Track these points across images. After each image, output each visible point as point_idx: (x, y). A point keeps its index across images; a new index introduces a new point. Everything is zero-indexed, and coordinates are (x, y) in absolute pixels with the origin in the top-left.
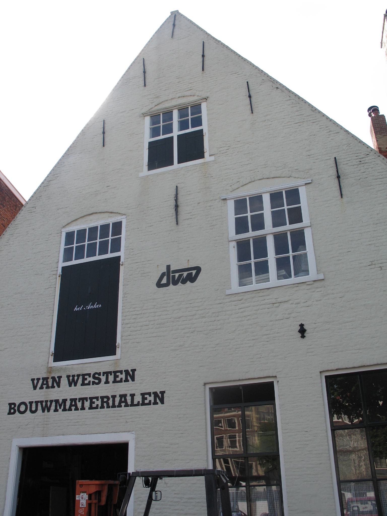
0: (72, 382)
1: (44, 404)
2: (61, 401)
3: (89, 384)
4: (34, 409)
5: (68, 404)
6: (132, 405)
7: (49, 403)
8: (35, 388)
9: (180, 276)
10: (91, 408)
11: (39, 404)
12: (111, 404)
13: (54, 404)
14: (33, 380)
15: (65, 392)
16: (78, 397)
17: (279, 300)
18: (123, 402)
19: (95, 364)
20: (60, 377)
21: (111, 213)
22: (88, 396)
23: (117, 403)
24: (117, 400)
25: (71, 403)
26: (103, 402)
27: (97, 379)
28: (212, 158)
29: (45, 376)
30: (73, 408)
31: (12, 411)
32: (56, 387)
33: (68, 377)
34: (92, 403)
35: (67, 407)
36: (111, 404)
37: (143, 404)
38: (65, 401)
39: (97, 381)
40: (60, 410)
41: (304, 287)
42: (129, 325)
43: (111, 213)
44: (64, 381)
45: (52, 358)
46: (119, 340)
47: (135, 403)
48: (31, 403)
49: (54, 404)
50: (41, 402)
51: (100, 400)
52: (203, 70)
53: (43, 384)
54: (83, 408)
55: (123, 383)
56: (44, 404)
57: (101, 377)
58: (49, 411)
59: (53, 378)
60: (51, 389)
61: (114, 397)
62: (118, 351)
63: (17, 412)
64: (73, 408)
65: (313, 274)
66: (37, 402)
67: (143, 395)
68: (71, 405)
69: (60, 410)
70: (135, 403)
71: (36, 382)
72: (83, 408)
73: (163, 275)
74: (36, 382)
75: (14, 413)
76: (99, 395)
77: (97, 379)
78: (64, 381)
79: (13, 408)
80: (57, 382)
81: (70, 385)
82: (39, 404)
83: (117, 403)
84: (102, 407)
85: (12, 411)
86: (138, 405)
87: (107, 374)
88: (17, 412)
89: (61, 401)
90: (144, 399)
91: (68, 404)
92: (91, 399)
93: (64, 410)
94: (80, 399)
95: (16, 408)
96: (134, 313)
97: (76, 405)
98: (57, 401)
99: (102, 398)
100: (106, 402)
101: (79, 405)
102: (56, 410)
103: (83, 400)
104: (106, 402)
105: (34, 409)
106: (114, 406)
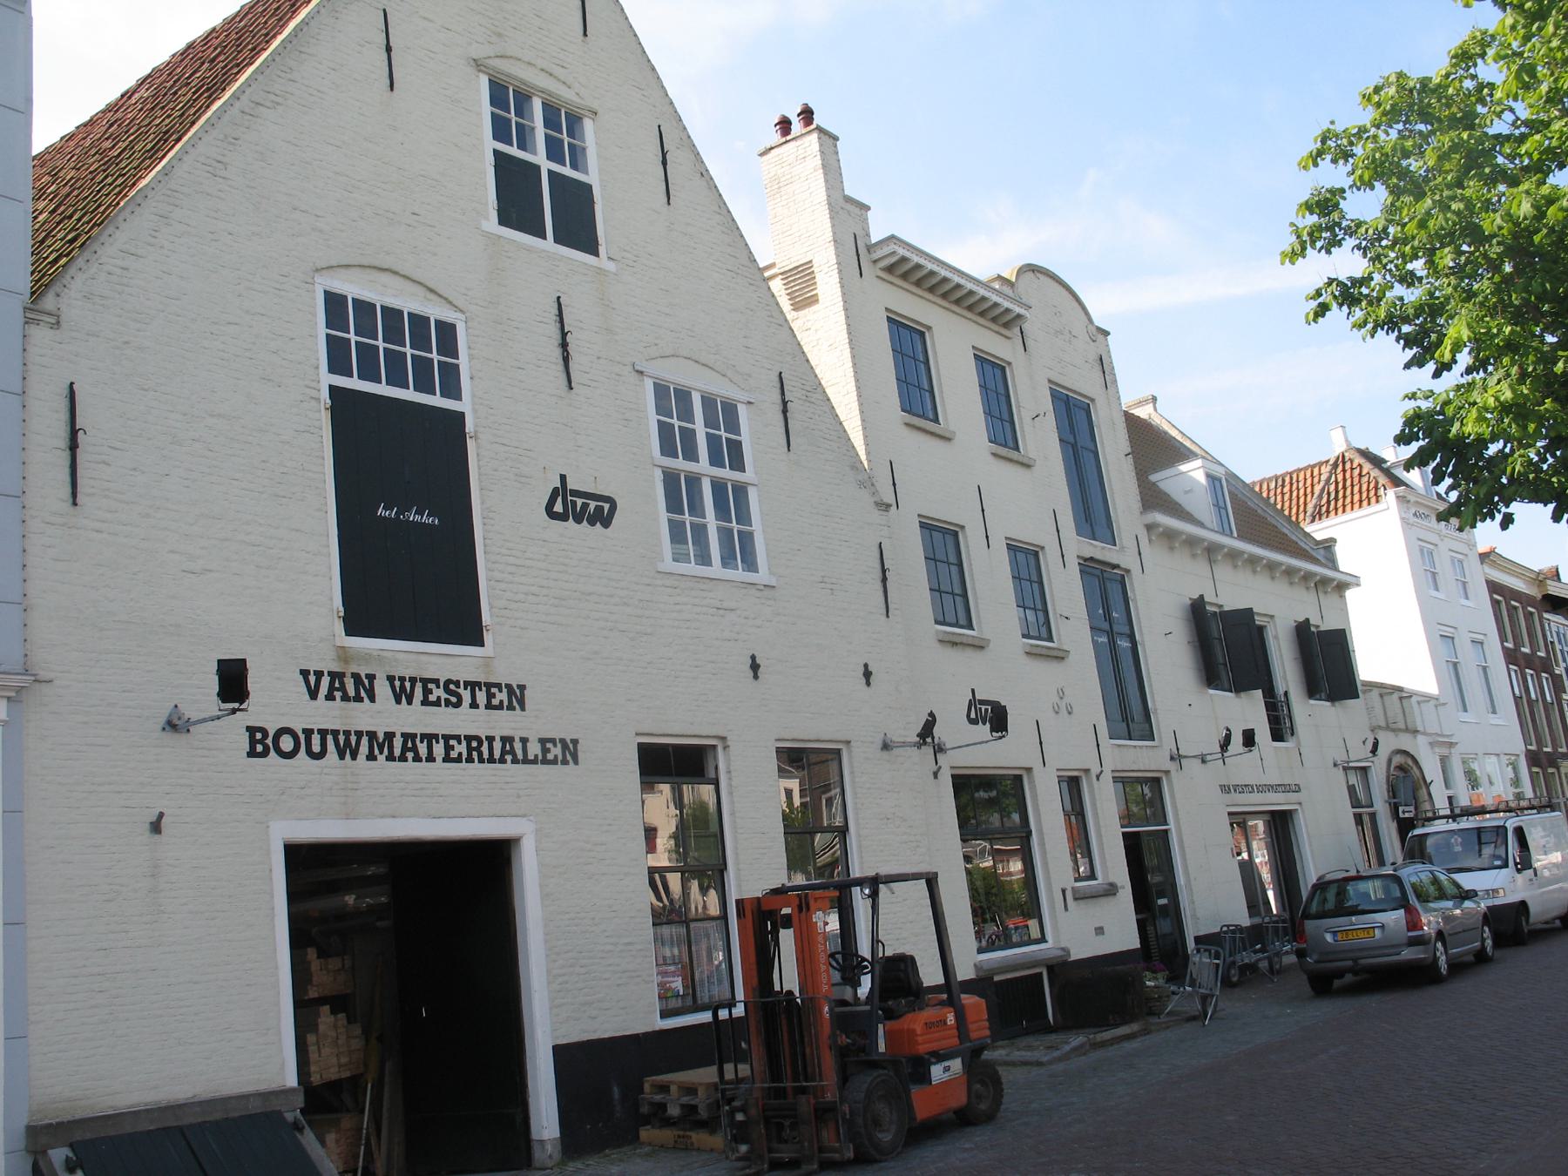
0: (402, 693)
1: (342, 738)
2: (381, 737)
3: (437, 703)
4: (316, 748)
5: (398, 743)
6: (526, 761)
7: (353, 739)
8: (313, 695)
9: (585, 506)
10: (447, 759)
11: (330, 738)
12: (486, 755)
13: (365, 741)
14: (305, 673)
15: (383, 715)
16: (418, 731)
17: (725, 605)
18: (410, 750)
19: (444, 659)
20: (371, 677)
21: (431, 291)
22: (441, 732)
23: (497, 754)
24: (497, 745)
25: (504, 747)
26: (470, 749)
27: (453, 692)
28: (611, 266)
29: (336, 668)
30: (410, 755)
31: (259, 748)
32: (366, 700)
33: (391, 679)
34: (448, 748)
35: (397, 752)
36: (486, 755)
37: (545, 761)
38: (390, 736)
39: (454, 700)
40: (381, 758)
41: (753, 591)
42: (503, 586)
43: (431, 291)
44: (382, 689)
45: (339, 627)
46: (486, 618)
47: (531, 757)
48: (308, 733)
49: (365, 741)
50: (335, 733)
51: (464, 743)
52: (585, 34)
53: (331, 688)
54: (431, 758)
55: (505, 712)
56: (342, 738)
57: (461, 691)
58: (354, 757)
59: (356, 677)
60: (353, 704)
61: (491, 739)
62: (488, 637)
63: (272, 753)
64: (410, 755)
65: (763, 575)
66: (323, 733)
67: (543, 741)
68: (405, 749)
69: (381, 758)
70: (531, 757)
71: (312, 679)
72: (431, 758)
73: (555, 494)
74: (312, 679)
75: (265, 754)
76: (462, 732)
77: (453, 692)
78: (382, 689)
79: (261, 741)
80: (365, 688)
81: (398, 702)
82: (330, 738)
83: (497, 754)
84: (470, 760)
85: (259, 748)
86: (534, 762)
87: (473, 686)
88: (272, 753)
89: (381, 737)
90: (545, 751)
91: (398, 743)
92: (447, 738)
93: (390, 758)
94: (423, 736)
95: (269, 741)
96: (512, 560)
97: (415, 749)
98: (372, 735)
99: (469, 739)
100: (476, 749)
101: (423, 749)
102: (371, 757)
103: (430, 738)
104: (476, 749)
105: (316, 748)
106: (491, 760)
